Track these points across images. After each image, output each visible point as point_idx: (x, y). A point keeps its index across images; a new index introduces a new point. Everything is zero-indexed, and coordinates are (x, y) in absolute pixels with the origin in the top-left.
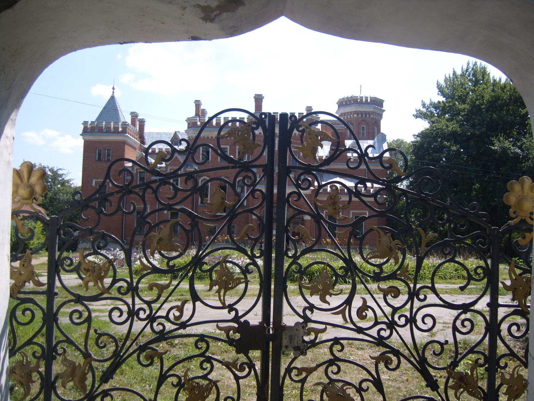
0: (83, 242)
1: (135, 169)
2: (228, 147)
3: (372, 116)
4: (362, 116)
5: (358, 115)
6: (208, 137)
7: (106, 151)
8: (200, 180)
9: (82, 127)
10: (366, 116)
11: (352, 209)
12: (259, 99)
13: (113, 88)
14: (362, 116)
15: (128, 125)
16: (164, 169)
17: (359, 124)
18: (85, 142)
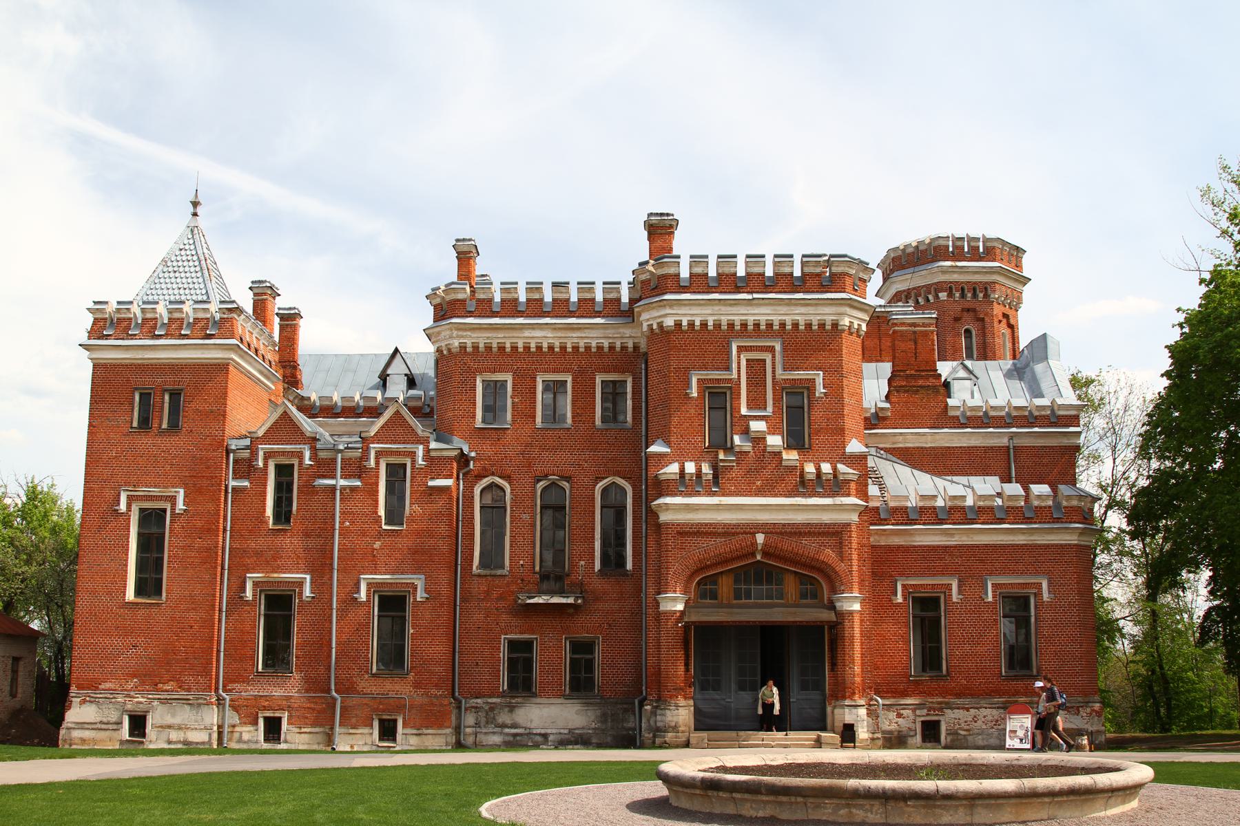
0: (83, 702)
1: (261, 454)
2: (569, 379)
4: (963, 296)
5: (950, 295)
6: (502, 348)
7: (167, 397)
8: (477, 490)
9: (89, 320)
10: (975, 295)
11: (991, 574)
12: (660, 230)
13: (195, 204)
14: (963, 296)
15: (239, 310)
16: (358, 453)
17: (957, 319)
18: (95, 366)
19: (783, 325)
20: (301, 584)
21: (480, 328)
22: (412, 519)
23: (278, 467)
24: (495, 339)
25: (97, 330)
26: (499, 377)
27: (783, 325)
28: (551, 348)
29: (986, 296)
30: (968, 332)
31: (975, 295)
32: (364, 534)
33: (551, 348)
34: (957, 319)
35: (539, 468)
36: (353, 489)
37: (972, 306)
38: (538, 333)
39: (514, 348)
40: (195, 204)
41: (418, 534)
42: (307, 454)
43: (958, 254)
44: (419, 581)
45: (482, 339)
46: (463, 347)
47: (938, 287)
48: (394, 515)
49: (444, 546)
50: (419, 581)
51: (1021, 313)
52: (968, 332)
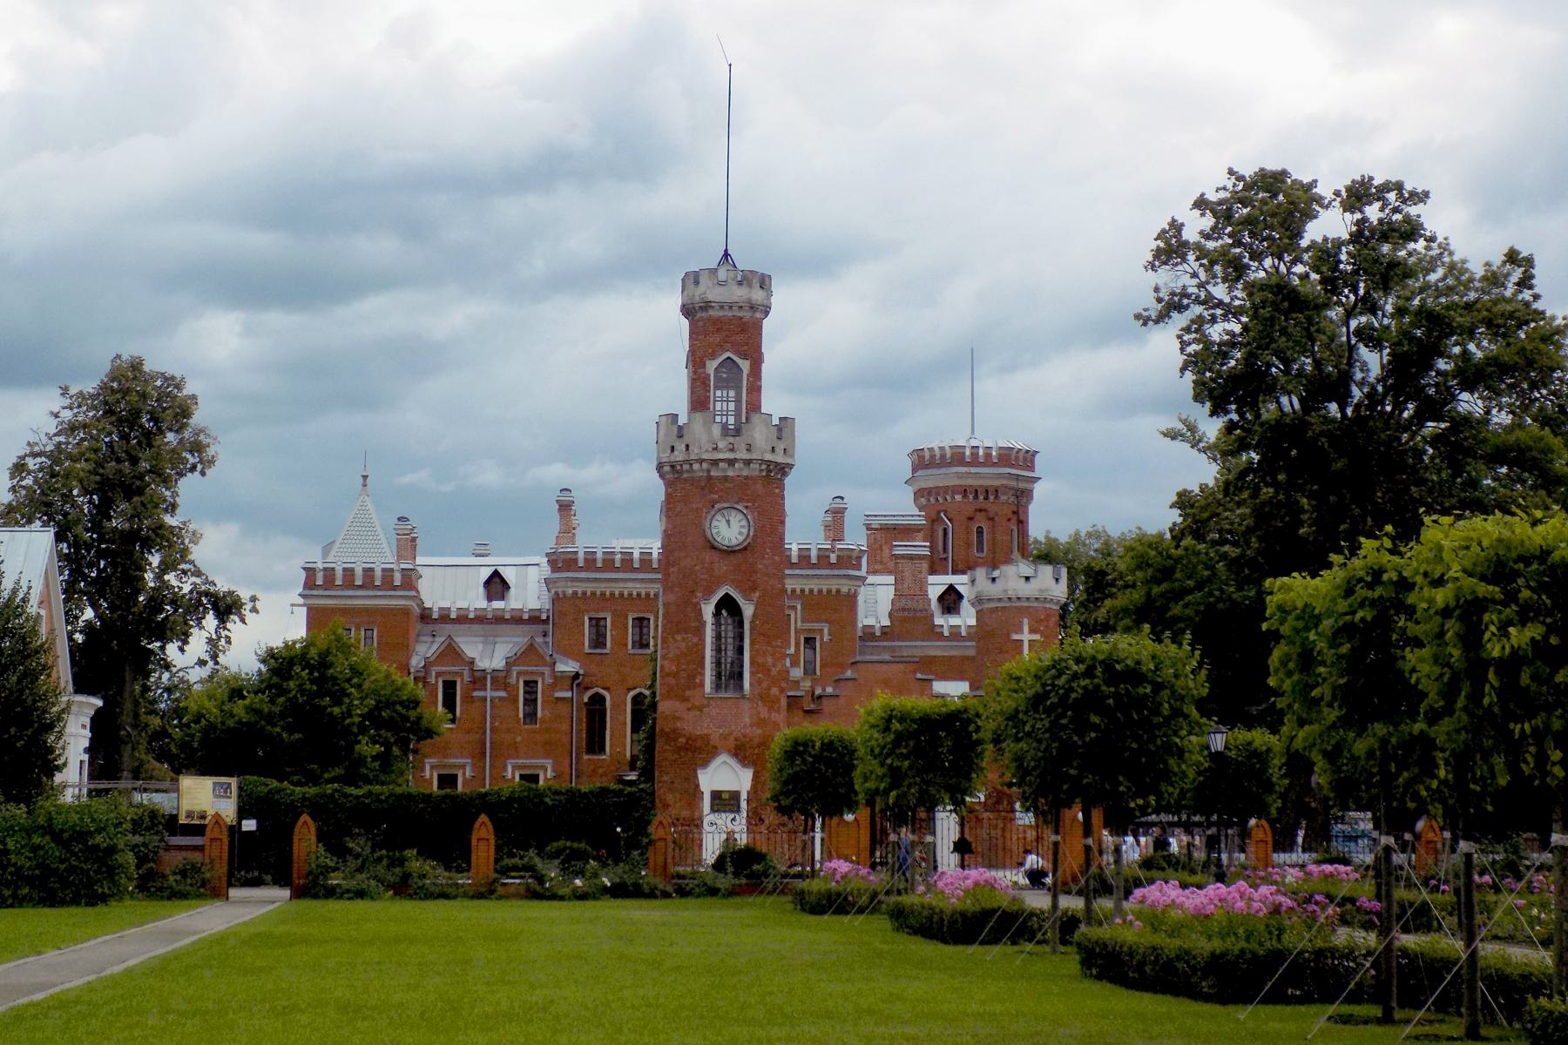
3: (1003, 498)
4: (976, 497)
6: (603, 594)
10: (986, 498)
13: (365, 477)
14: (976, 497)
17: (970, 519)
19: (802, 591)
20: (463, 767)
21: (588, 580)
22: (542, 721)
23: (445, 682)
24: (599, 588)
25: (310, 584)
26: (601, 615)
27: (802, 591)
28: (639, 595)
29: (996, 497)
30: (980, 531)
31: (986, 498)
32: (508, 731)
33: (639, 595)
34: (970, 519)
35: (630, 683)
36: (501, 699)
37: (984, 506)
38: (631, 585)
39: (612, 594)
40: (365, 477)
41: (547, 730)
42: (466, 673)
43: (975, 461)
44: (548, 763)
45: (589, 588)
46: (575, 593)
47: (954, 490)
48: (531, 716)
49: (566, 739)
50: (548, 763)
51: (1032, 508)
52: (980, 531)
